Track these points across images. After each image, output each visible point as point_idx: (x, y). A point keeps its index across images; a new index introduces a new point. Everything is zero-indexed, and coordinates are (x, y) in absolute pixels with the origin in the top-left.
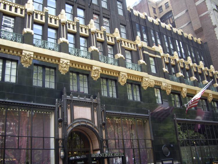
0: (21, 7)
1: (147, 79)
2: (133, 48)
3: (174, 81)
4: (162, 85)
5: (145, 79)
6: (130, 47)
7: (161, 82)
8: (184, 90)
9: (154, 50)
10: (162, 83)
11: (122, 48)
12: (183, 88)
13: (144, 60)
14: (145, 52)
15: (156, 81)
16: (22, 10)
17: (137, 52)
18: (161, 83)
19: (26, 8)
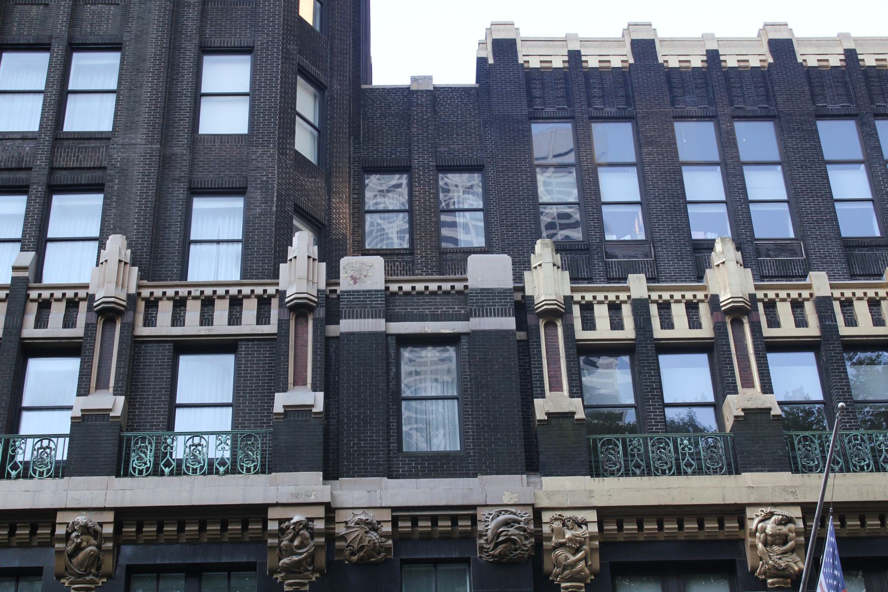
0: (170, 292)
1: (298, 517)
2: (249, 324)
3: (648, 472)
4: (480, 527)
5: (281, 521)
6: (221, 325)
7: (474, 507)
8: (752, 525)
9: (459, 286)
10: (481, 513)
11: (136, 347)
12: (750, 513)
13: (326, 382)
14: (347, 325)
15: (398, 513)
16: (264, 302)
17: (274, 344)
18: (474, 519)
19: (281, 288)
